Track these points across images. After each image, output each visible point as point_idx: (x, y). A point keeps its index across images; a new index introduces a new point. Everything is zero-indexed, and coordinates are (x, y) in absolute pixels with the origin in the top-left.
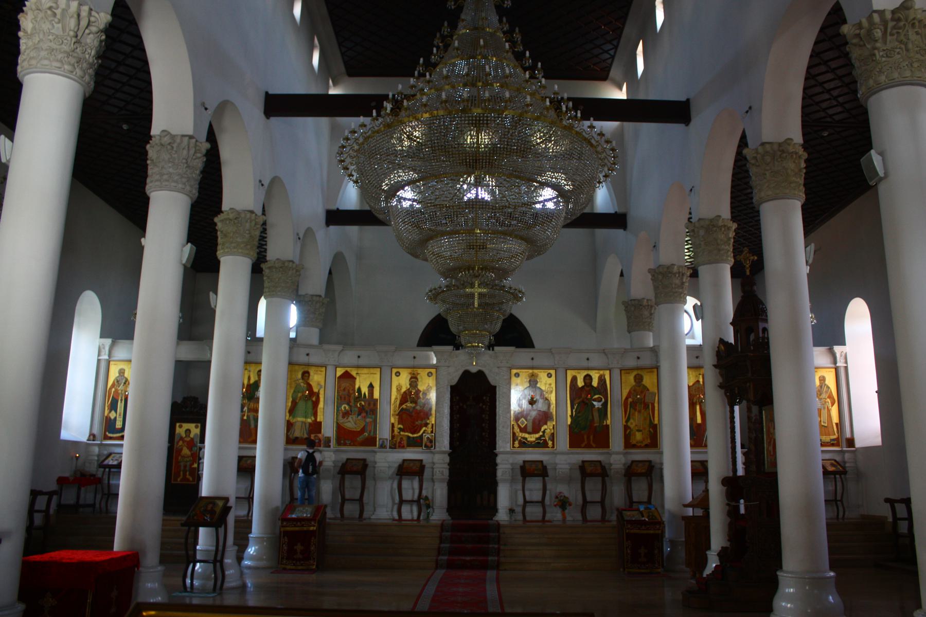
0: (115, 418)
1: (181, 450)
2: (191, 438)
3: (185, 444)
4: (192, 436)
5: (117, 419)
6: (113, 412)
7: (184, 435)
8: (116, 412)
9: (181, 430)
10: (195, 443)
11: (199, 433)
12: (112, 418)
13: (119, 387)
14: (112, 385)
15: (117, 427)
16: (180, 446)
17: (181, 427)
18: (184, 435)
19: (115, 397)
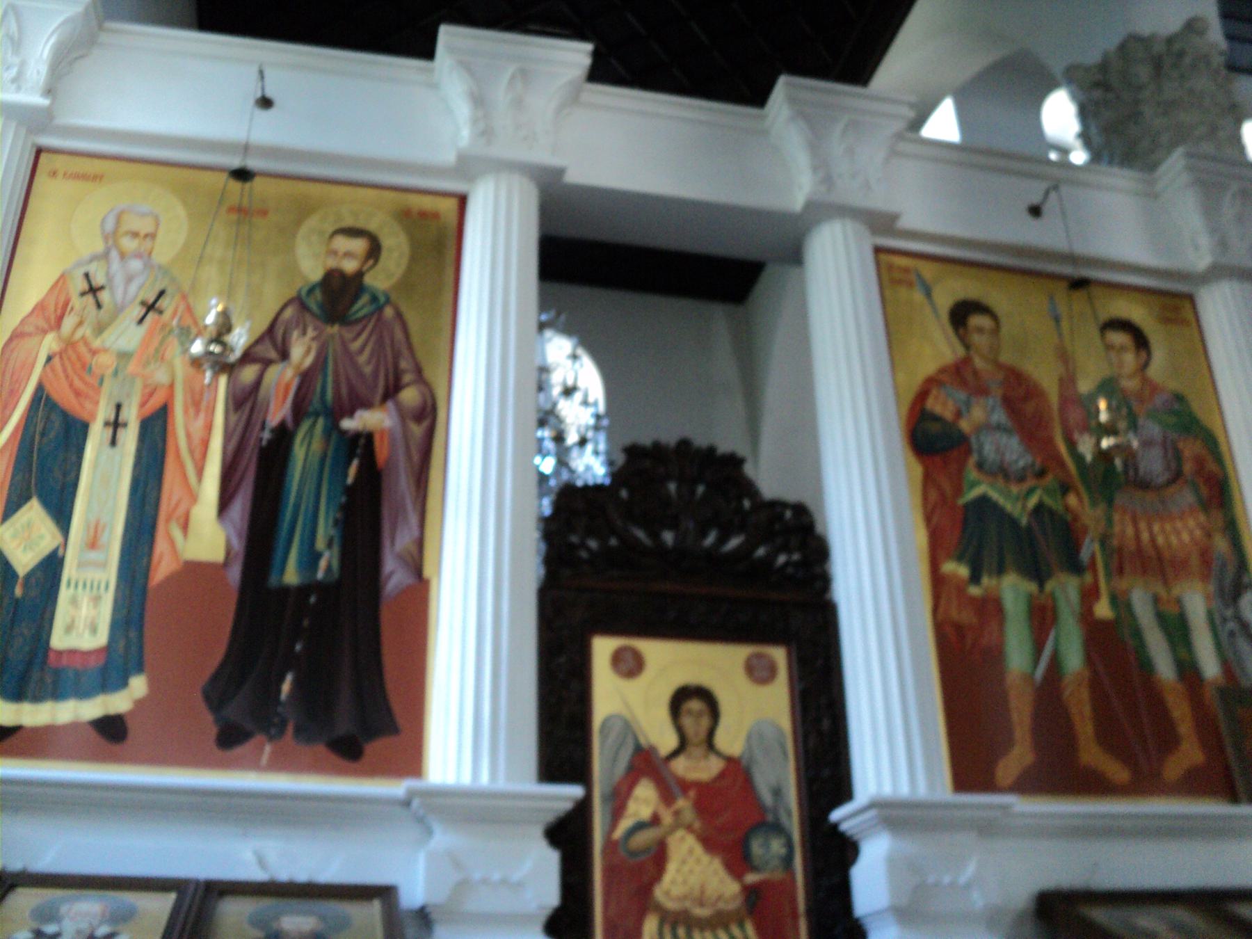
0: (52, 566)
1: (659, 856)
2: (731, 761)
3: (682, 803)
4: (730, 739)
5: (69, 571)
6: (34, 513)
7: (664, 738)
8: (61, 514)
9: (633, 689)
10: (767, 798)
11: (785, 722)
12: (24, 560)
13: (100, 329)
14: (40, 307)
15: (59, 640)
16: (640, 826)
17: (629, 665)
18: (664, 738)
19: (62, 395)
